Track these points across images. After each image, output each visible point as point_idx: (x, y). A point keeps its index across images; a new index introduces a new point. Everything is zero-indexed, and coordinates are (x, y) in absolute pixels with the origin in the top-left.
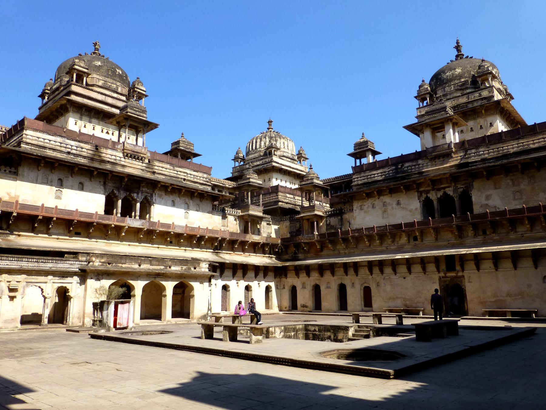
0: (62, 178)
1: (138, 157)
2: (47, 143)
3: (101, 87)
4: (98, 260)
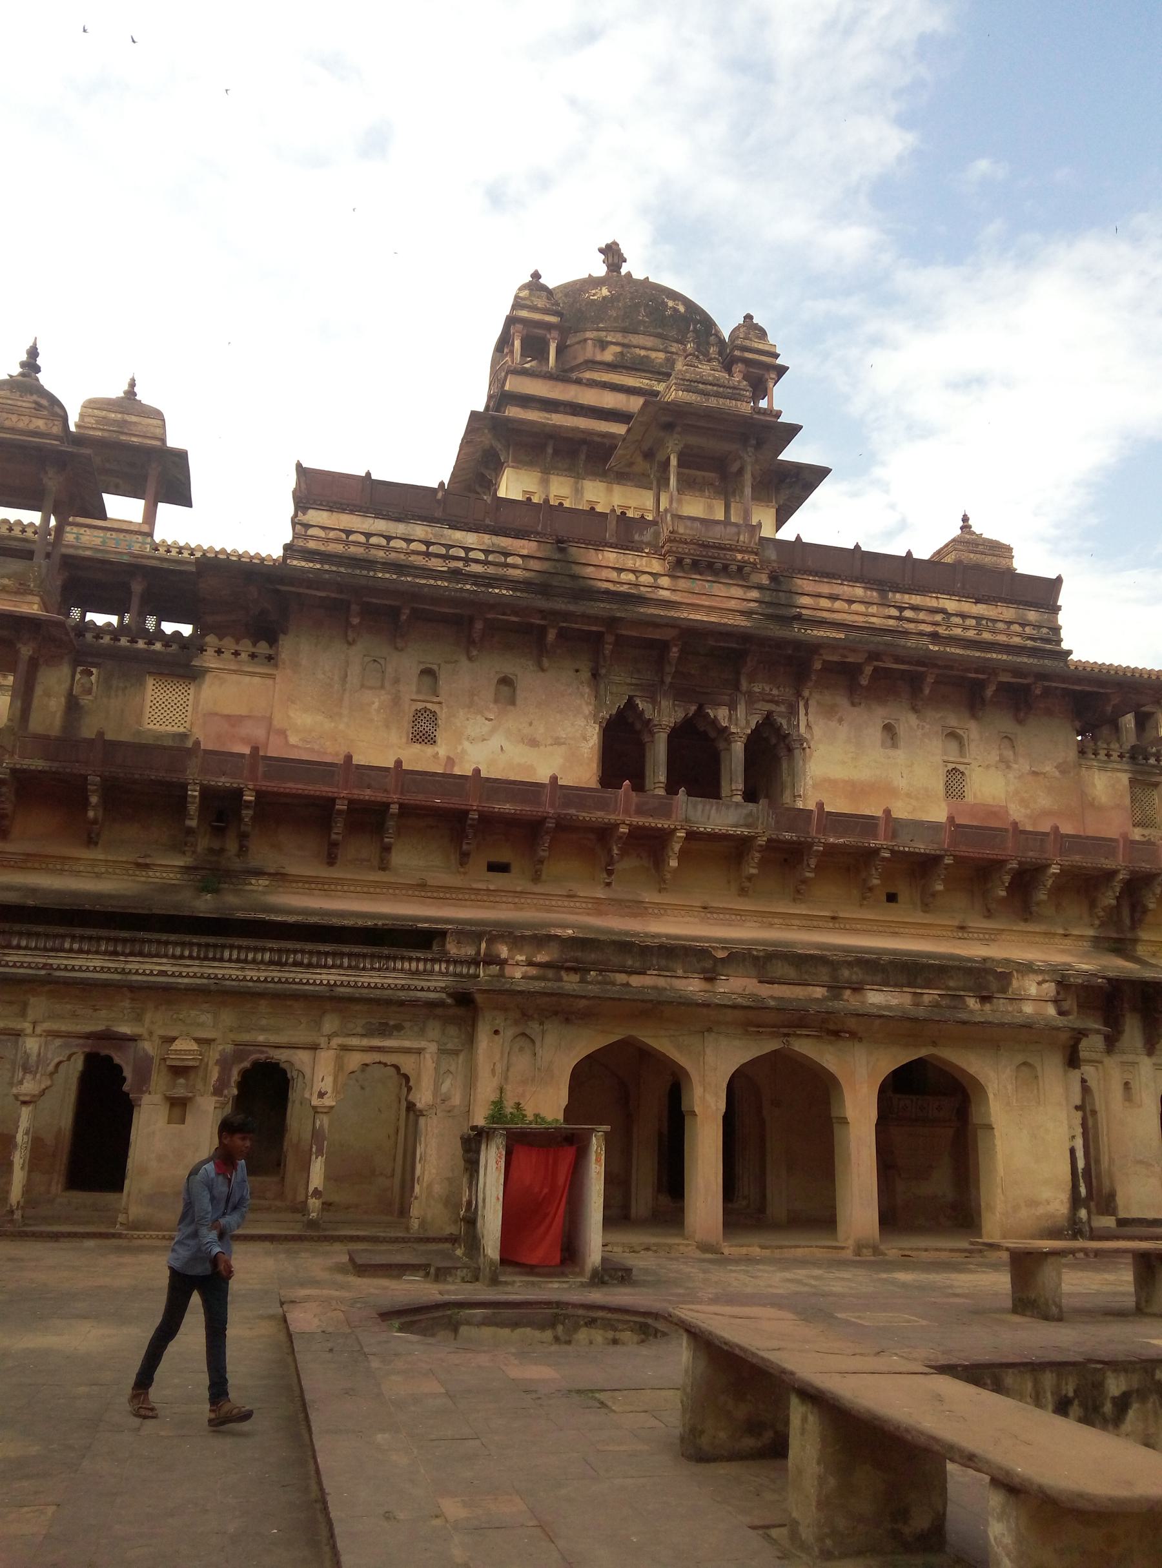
0: (435, 667)
1: (725, 568)
2: (378, 547)
3: (611, 367)
4: (520, 958)
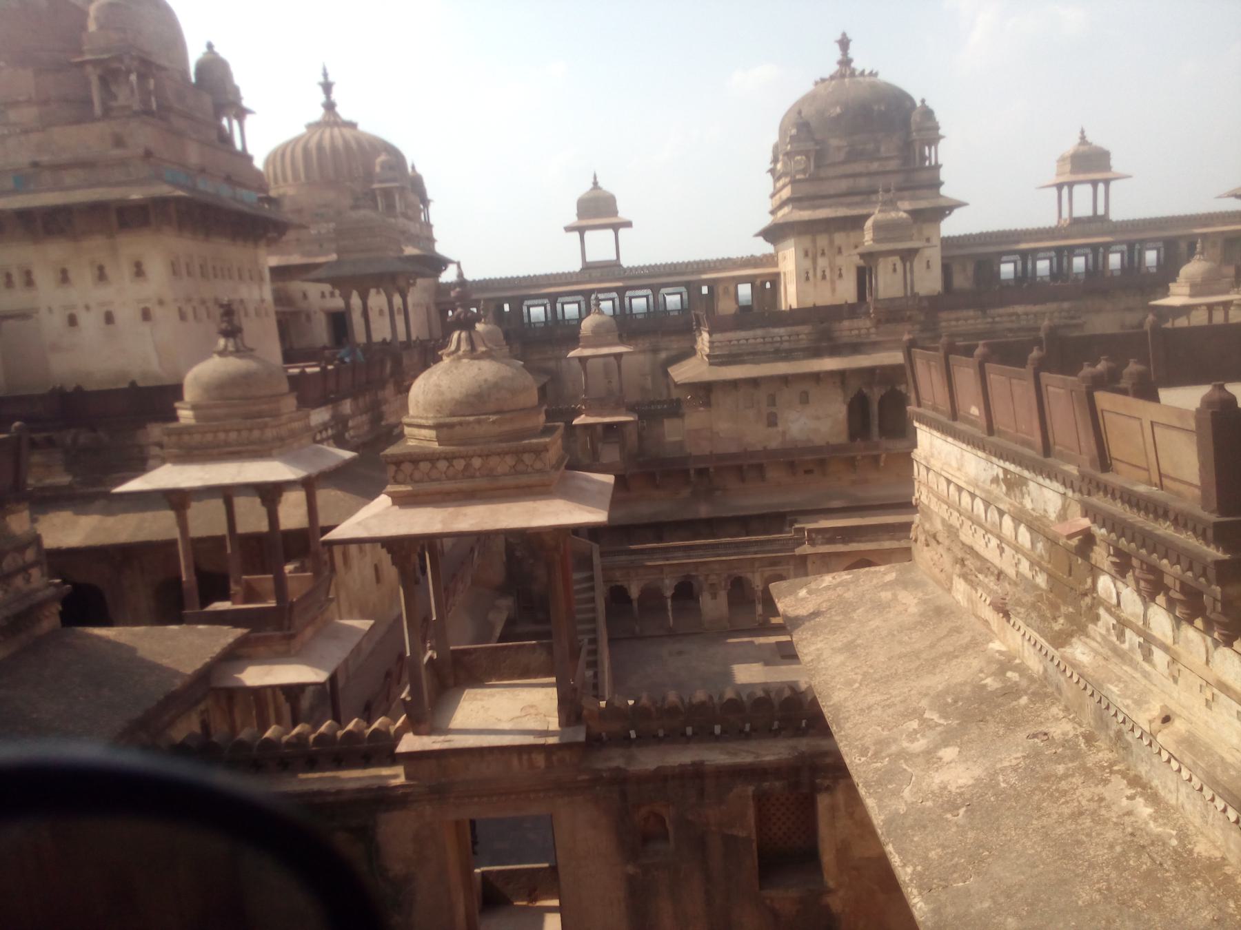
4: (820, 537)
